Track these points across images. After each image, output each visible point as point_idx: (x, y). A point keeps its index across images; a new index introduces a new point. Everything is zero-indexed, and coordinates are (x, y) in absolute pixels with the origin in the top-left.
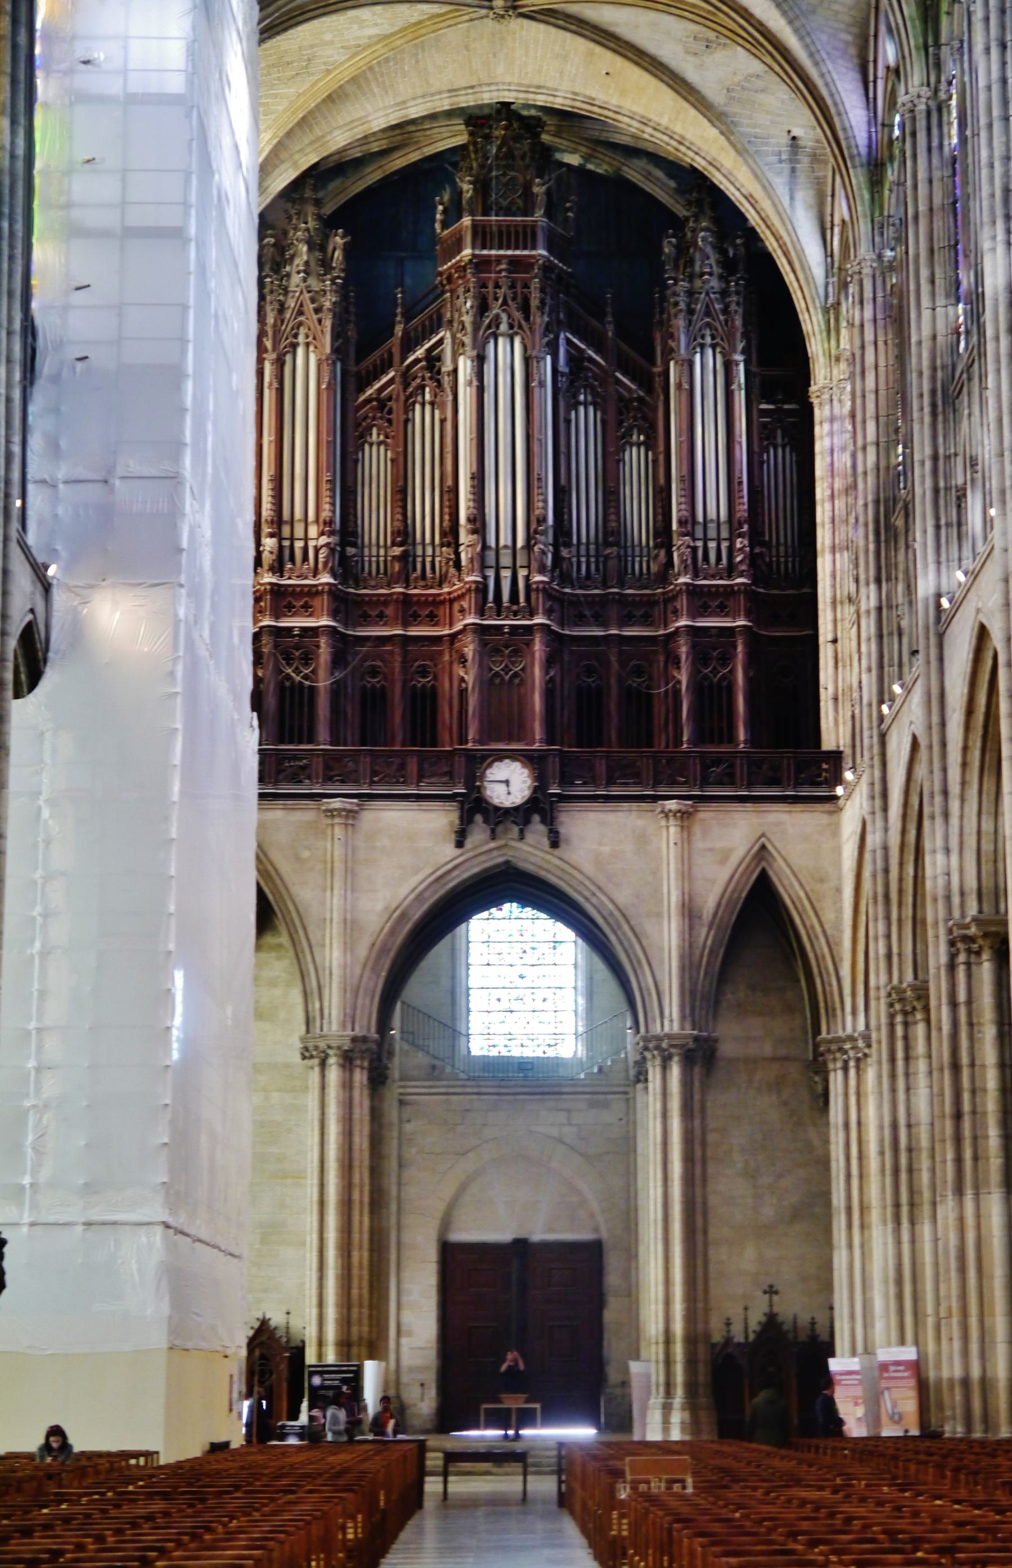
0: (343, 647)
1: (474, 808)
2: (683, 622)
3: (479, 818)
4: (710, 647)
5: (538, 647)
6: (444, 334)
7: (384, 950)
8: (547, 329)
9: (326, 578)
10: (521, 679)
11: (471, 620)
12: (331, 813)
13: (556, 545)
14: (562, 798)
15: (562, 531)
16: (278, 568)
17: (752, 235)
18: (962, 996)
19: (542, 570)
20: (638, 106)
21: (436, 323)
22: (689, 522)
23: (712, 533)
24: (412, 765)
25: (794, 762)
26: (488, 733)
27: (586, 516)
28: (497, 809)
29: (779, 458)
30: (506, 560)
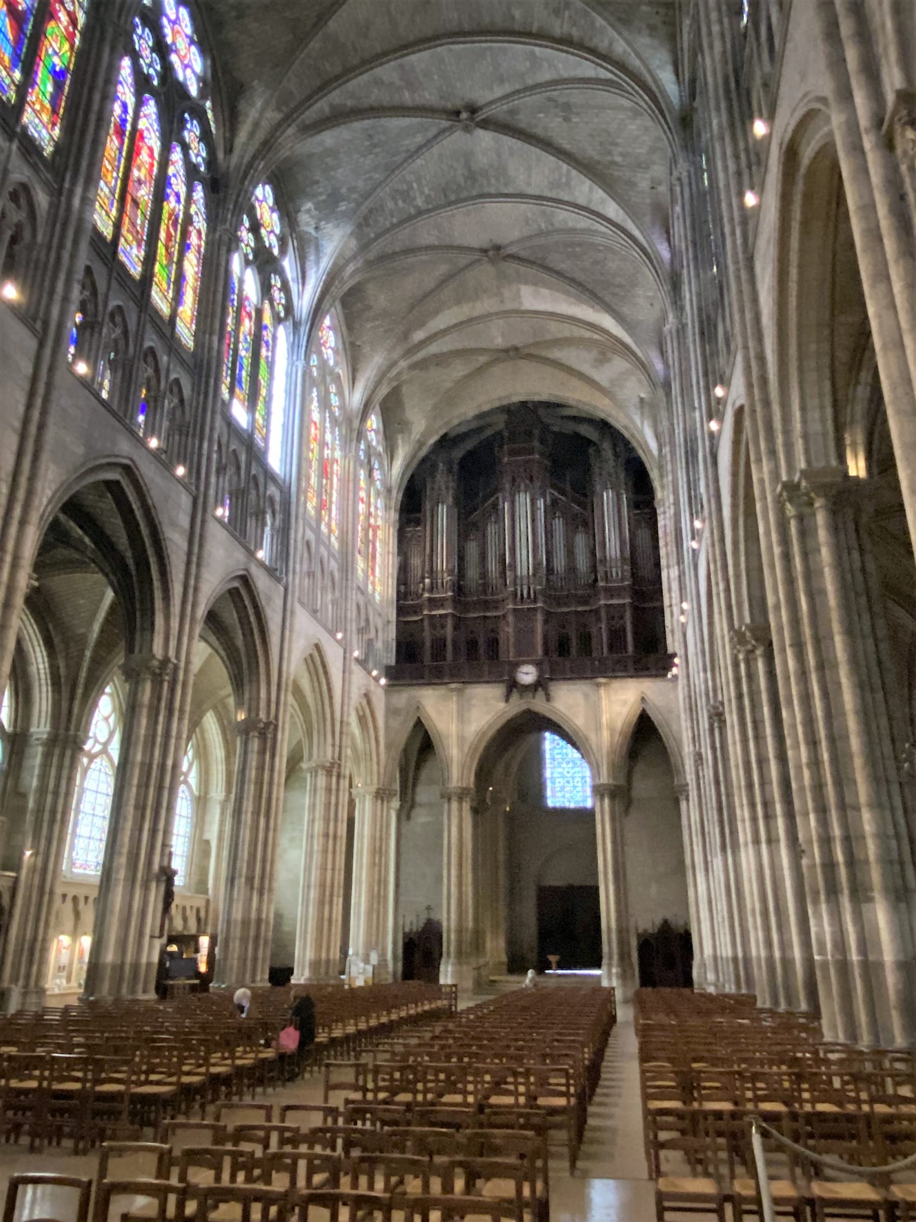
0: (459, 621)
1: (513, 686)
2: (602, 602)
3: (515, 690)
4: (614, 613)
5: (540, 617)
6: (500, 495)
7: (475, 749)
8: (541, 487)
9: (450, 594)
10: (533, 631)
11: (511, 606)
12: (452, 690)
13: (547, 575)
14: (551, 679)
15: (550, 570)
16: (431, 590)
17: (627, 443)
18: (718, 745)
19: (541, 584)
20: (577, 396)
21: (497, 490)
22: (604, 560)
23: (613, 564)
24: (486, 668)
25: (648, 651)
26: (519, 653)
27: (560, 563)
28: (522, 685)
29: (643, 534)
30: (525, 581)
